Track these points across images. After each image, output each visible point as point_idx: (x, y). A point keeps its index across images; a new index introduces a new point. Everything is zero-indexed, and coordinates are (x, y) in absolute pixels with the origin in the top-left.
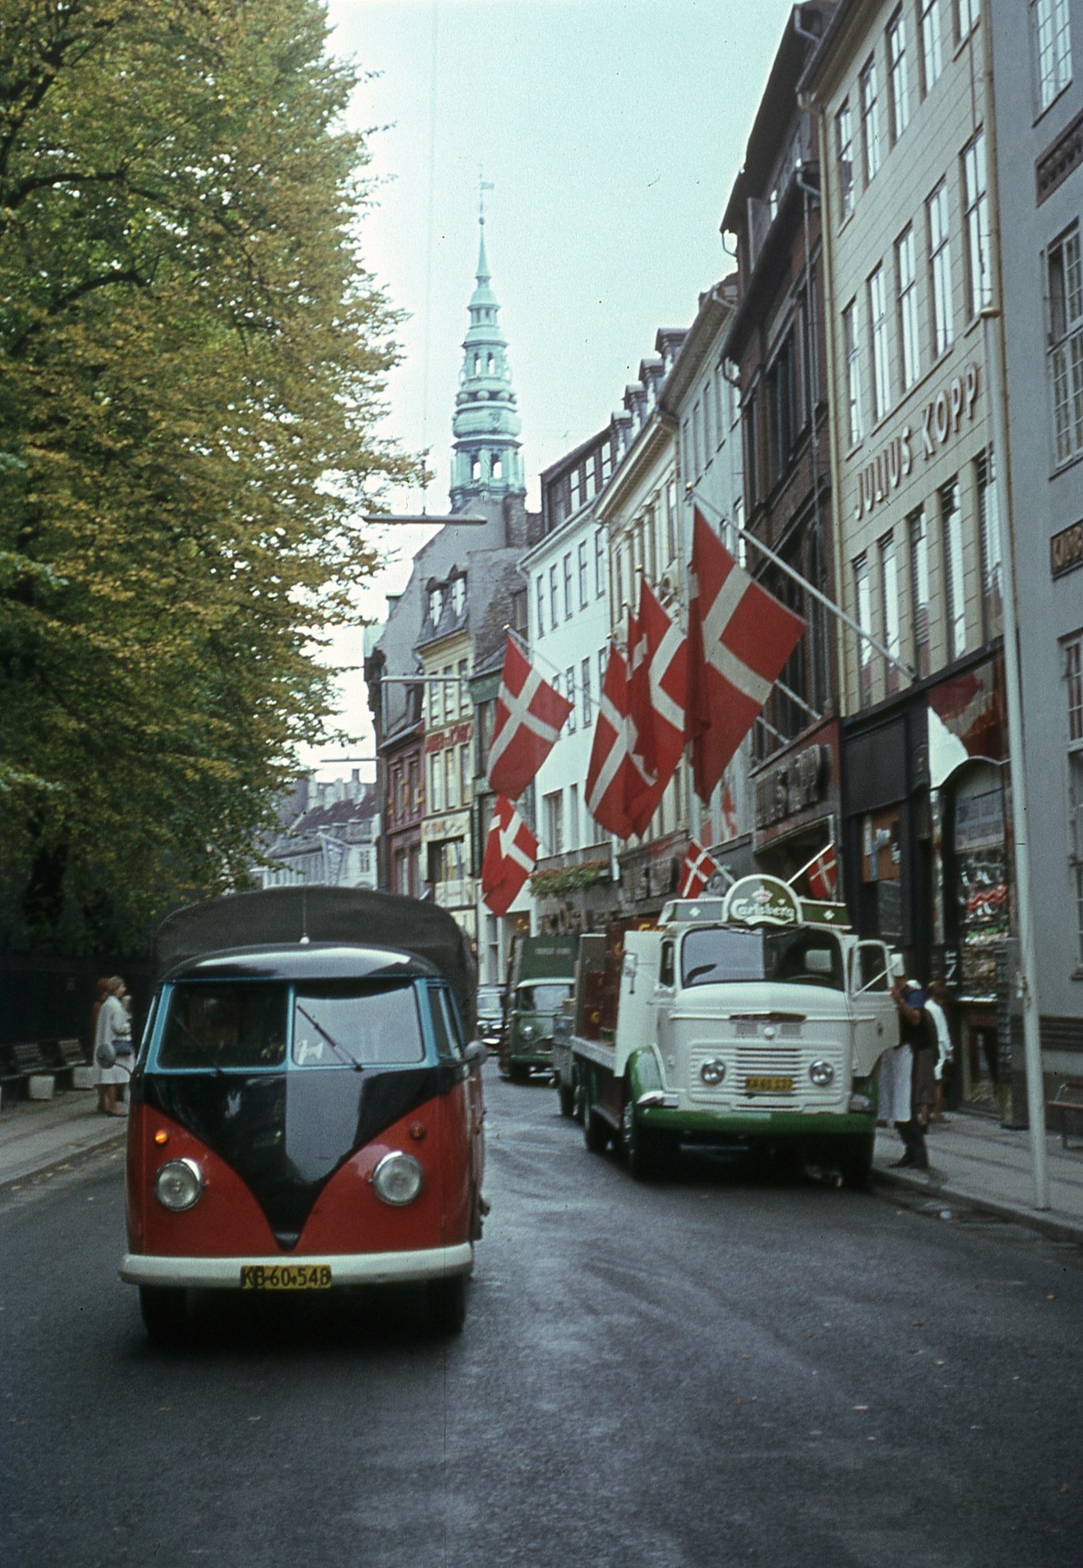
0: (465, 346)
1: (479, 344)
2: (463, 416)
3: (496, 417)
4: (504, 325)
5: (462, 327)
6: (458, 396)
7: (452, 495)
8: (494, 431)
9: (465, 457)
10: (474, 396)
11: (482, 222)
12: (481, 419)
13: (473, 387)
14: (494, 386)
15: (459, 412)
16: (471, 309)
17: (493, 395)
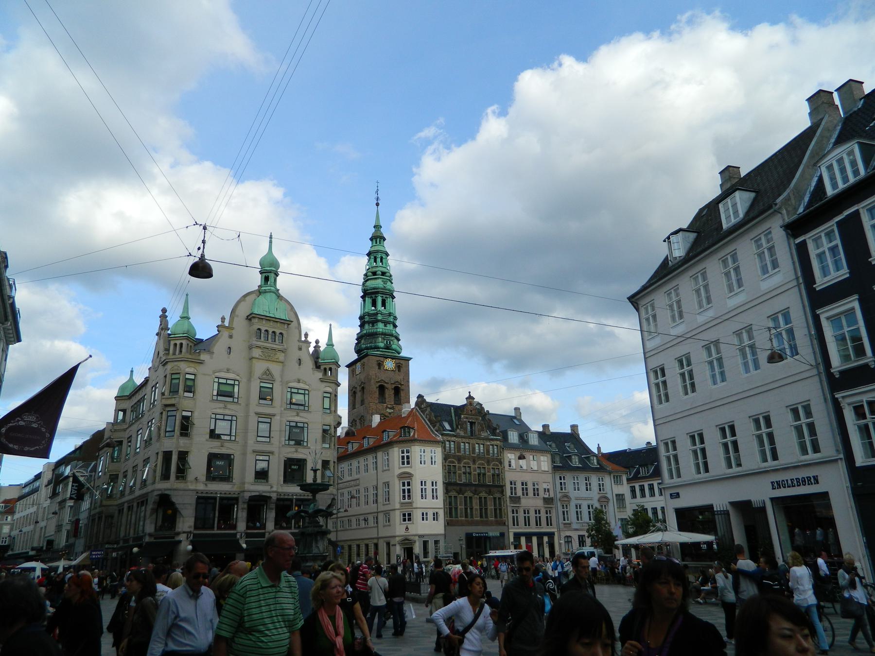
0: (369, 254)
1: (377, 251)
2: (368, 283)
3: (385, 283)
4: (387, 246)
5: (368, 246)
6: (366, 275)
7: (361, 318)
8: (384, 288)
9: (369, 301)
10: (374, 273)
11: (377, 204)
12: (378, 283)
13: (374, 270)
14: (384, 270)
15: (366, 281)
16: (371, 239)
17: (383, 274)
